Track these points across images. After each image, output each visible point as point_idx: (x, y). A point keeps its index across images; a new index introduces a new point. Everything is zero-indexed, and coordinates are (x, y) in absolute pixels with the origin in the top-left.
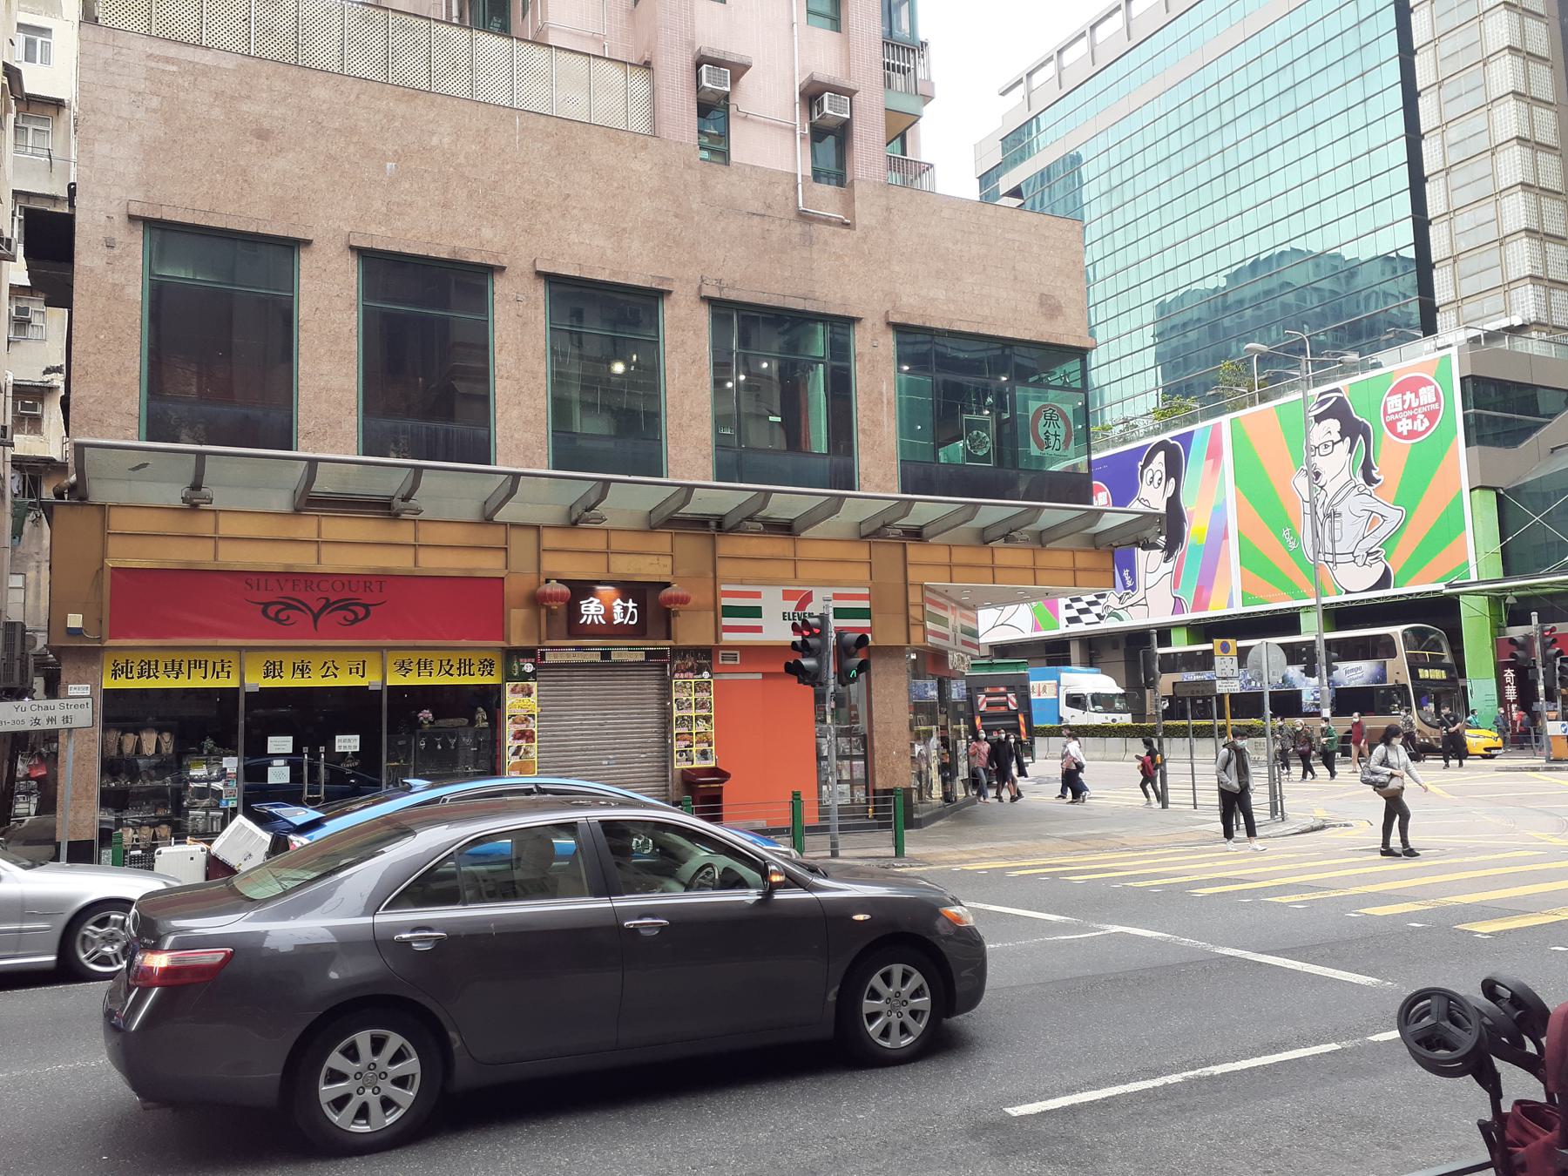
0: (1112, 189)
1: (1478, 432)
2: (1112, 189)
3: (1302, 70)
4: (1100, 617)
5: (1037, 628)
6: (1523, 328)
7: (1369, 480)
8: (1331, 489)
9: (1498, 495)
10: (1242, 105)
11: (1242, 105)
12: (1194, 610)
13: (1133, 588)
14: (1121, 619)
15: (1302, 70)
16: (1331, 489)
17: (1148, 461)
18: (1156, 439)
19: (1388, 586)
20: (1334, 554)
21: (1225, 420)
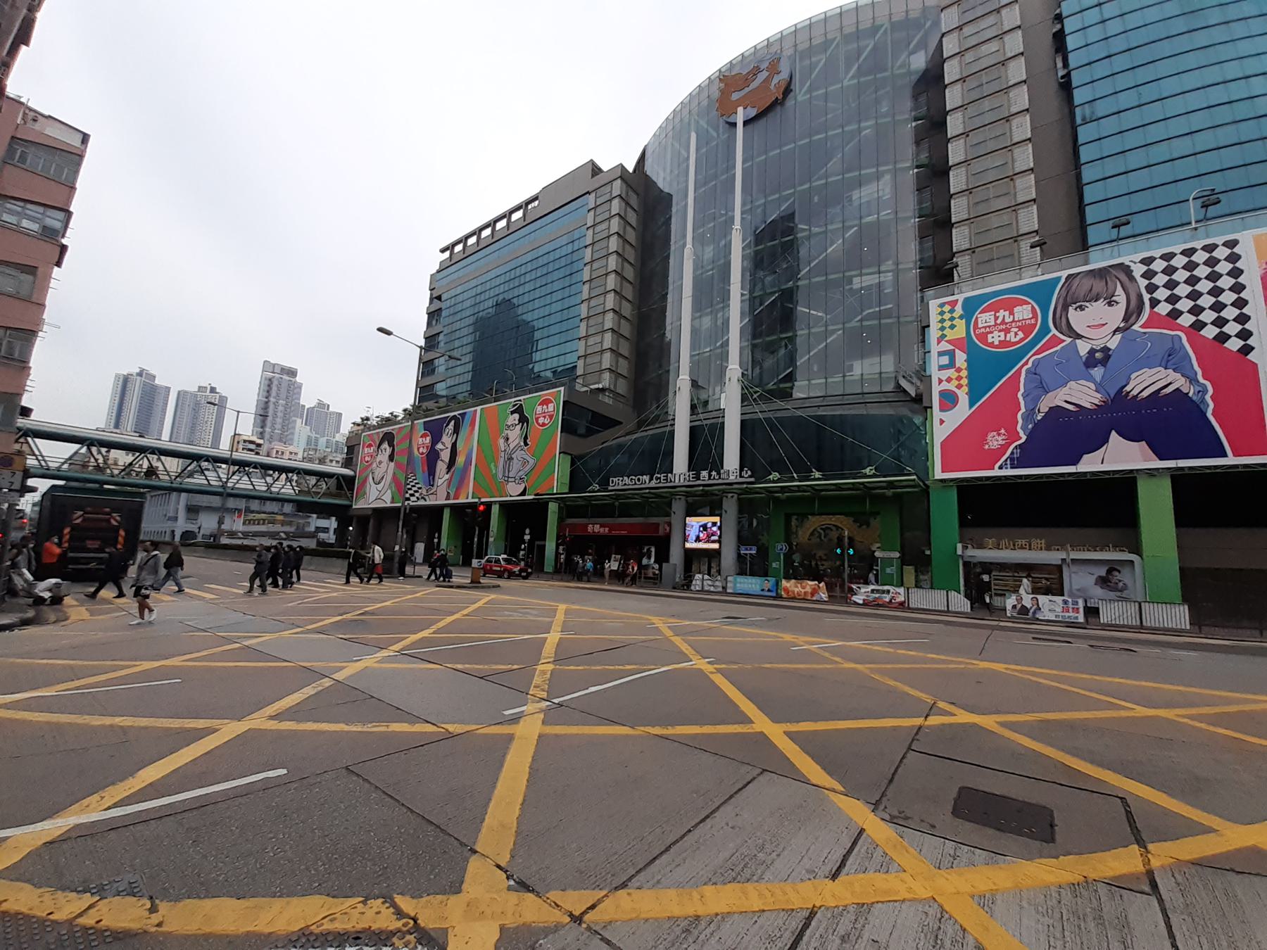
0: (476, 304)
1: (567, 428)
2: (476, 304)
3: (551, 267)
4: (418, 498)
5: (392, 502)
6: (602, 390)
7: (526, 444)
8: (512, 446)
9: (572, 458)
10: (528, 277)
11: (528, 277)
12: (454, 499)
13: (433, 486)
14: (425, 500)
15: (551, 267)
16: (512, 446)
17: (448, 425)
18: (452, 414)
19: (525, 495)
20: (508, 477)
21: (479, 408)
